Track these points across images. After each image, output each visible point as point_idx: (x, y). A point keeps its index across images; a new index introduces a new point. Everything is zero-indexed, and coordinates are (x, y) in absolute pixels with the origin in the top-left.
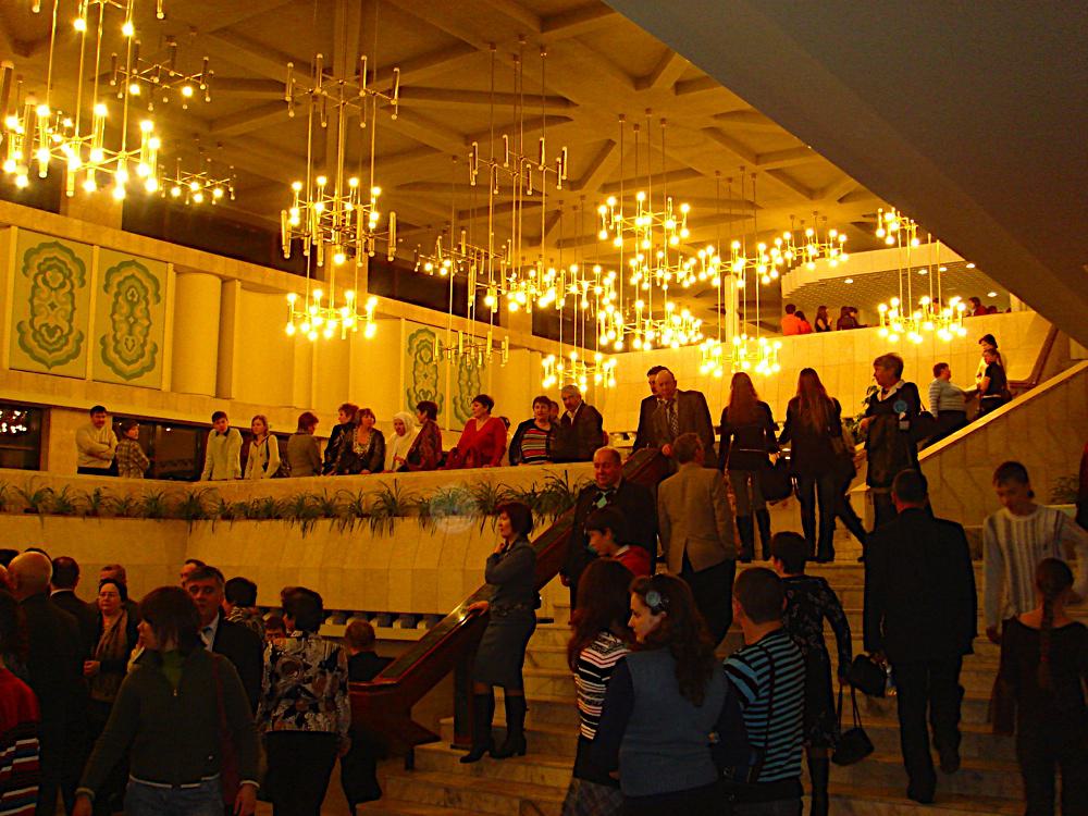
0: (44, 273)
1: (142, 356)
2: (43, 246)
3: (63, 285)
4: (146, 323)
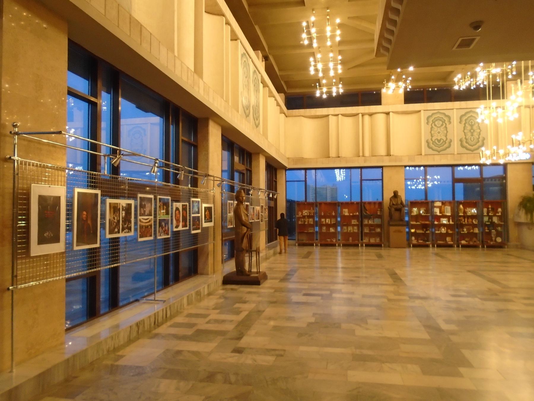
0: (434, 122)
1: (478, 142)
2: (433, 114)
3: (442, 125)
4: (479, 131)
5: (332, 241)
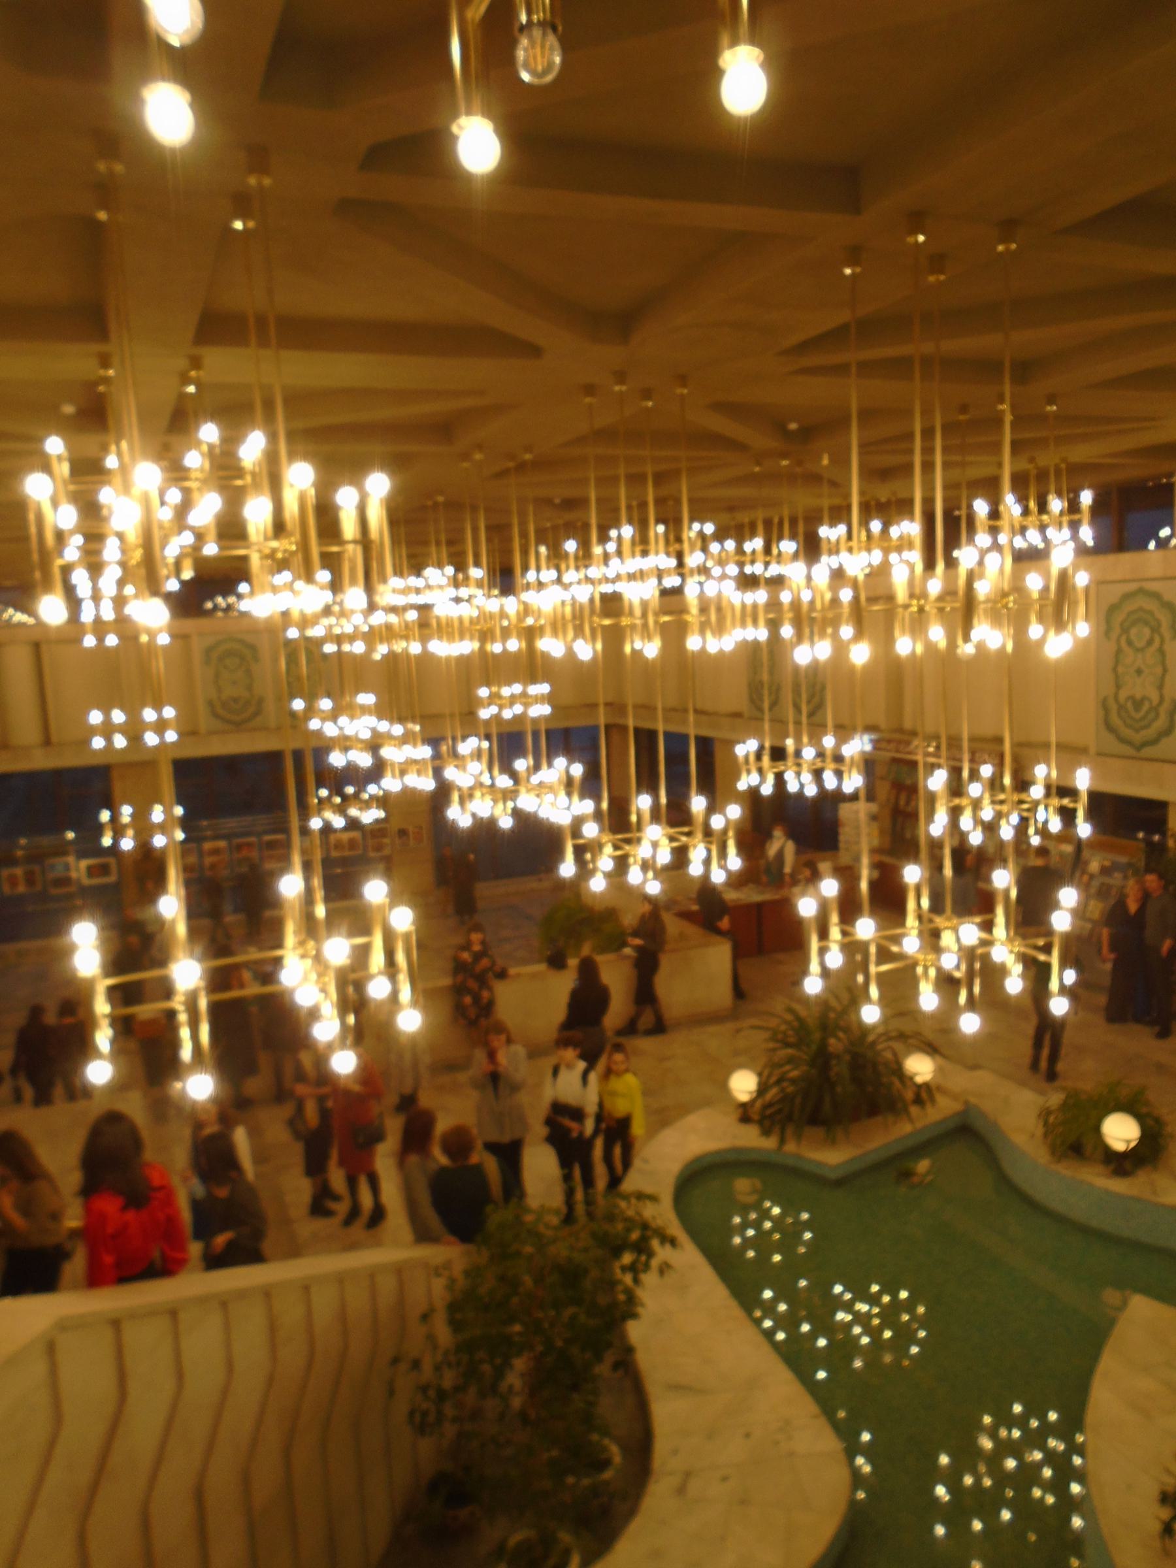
2: (1127, 597)
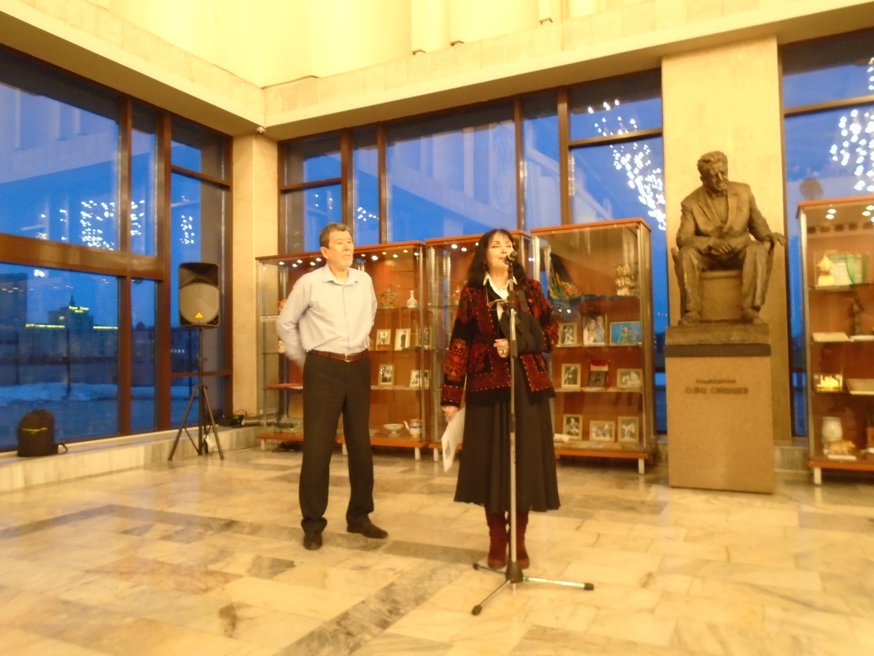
5: (404, 433)
